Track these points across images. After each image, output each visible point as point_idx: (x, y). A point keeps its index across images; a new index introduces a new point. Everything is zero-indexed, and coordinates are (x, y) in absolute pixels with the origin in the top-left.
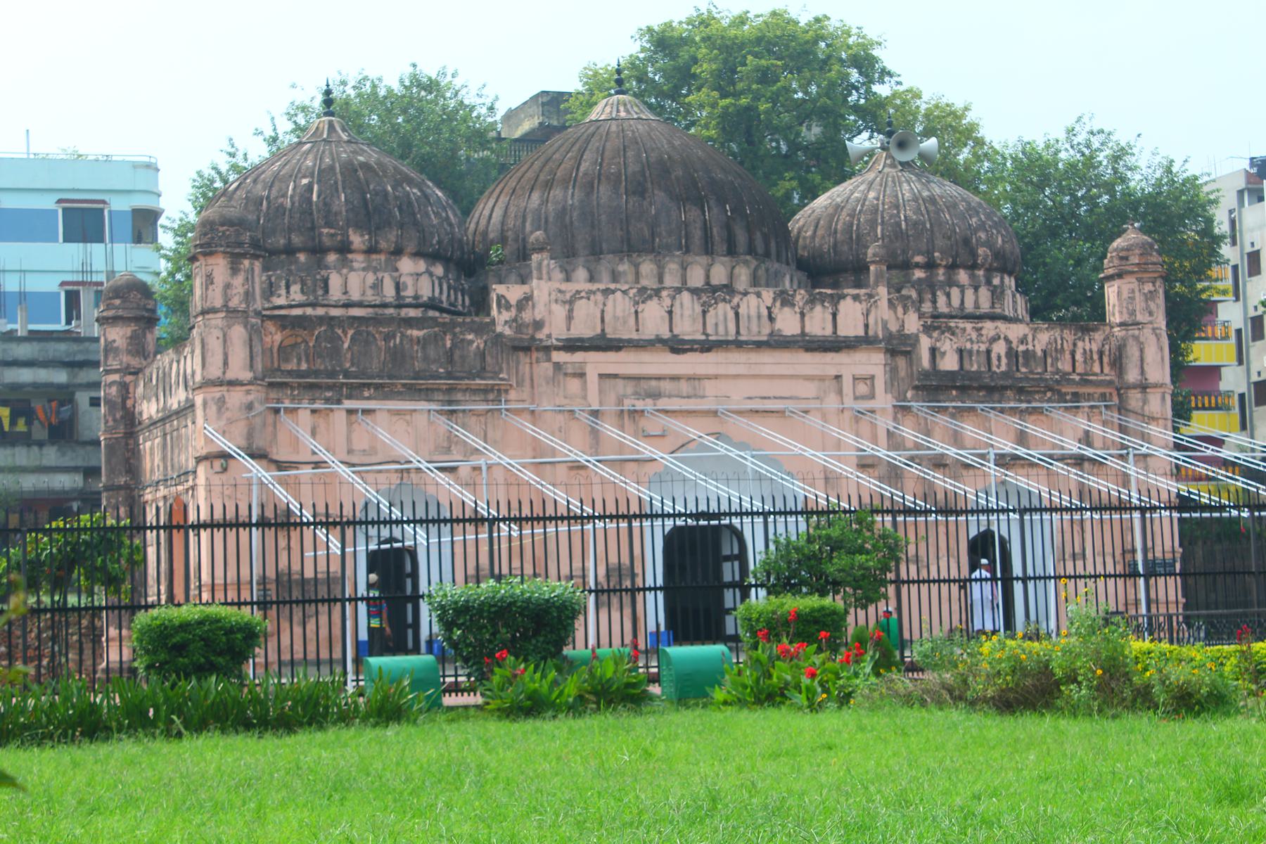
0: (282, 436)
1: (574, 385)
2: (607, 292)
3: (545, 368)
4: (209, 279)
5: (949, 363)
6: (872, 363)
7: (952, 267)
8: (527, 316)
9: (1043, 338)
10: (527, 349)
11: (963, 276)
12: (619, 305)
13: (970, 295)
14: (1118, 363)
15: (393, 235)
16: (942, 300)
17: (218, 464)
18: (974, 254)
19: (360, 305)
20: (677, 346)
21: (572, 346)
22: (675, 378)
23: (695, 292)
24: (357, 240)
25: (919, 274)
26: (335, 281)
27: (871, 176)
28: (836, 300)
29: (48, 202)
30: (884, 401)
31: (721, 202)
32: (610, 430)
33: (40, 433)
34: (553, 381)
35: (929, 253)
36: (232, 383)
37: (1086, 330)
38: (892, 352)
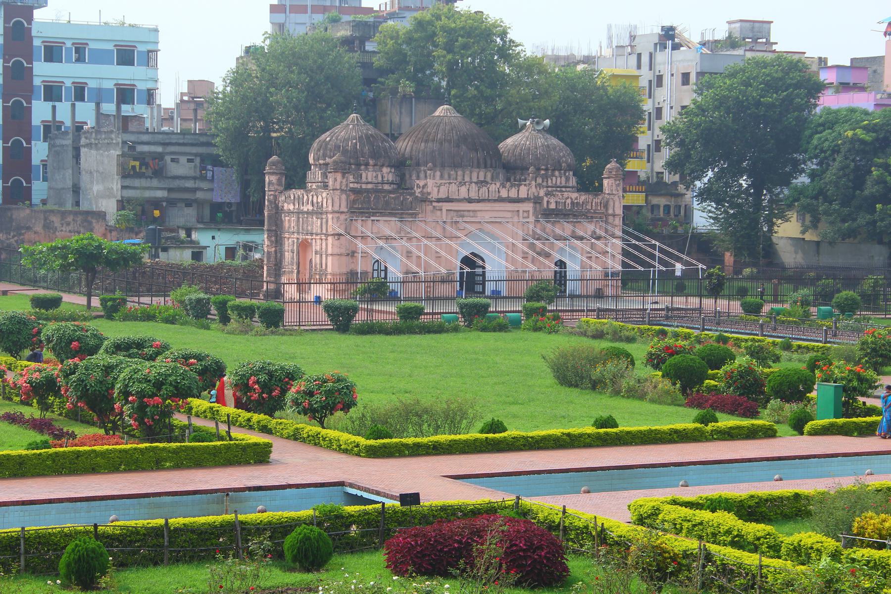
0: (353, 228)
1: (439, 213)
2: (450, 183)
3: (430, 208)
4: (336, 180)
5: (553, 206)
6: (529, 206)
7: (554, 170)
8: (425, 190)
9: (583, 197)
10: (425, 201)
11: (557, 173)
12: (453, 187)
13: (559, 179)
14: (606, 206)
15: (382, 160)
16: (550, 181)
17: (336, 237)
18: (561, 166)
19: (371, 183)
20: (470, 201)
21: (439, 200)
22: (469, 211)
23: (476, 183)
24: (371, 162)
25: (543, 172)
26: (364, 175)
27: (527, 134)
28: (519, 185)
29: (110, 46)
30: (532, 219)
31: (483, 151)
32: (448, 228)
33: (149, 172)
34: (432, 212)
35: (547, 166)
36: (342, 213)
37: (596, 195)
38: (535, 203)
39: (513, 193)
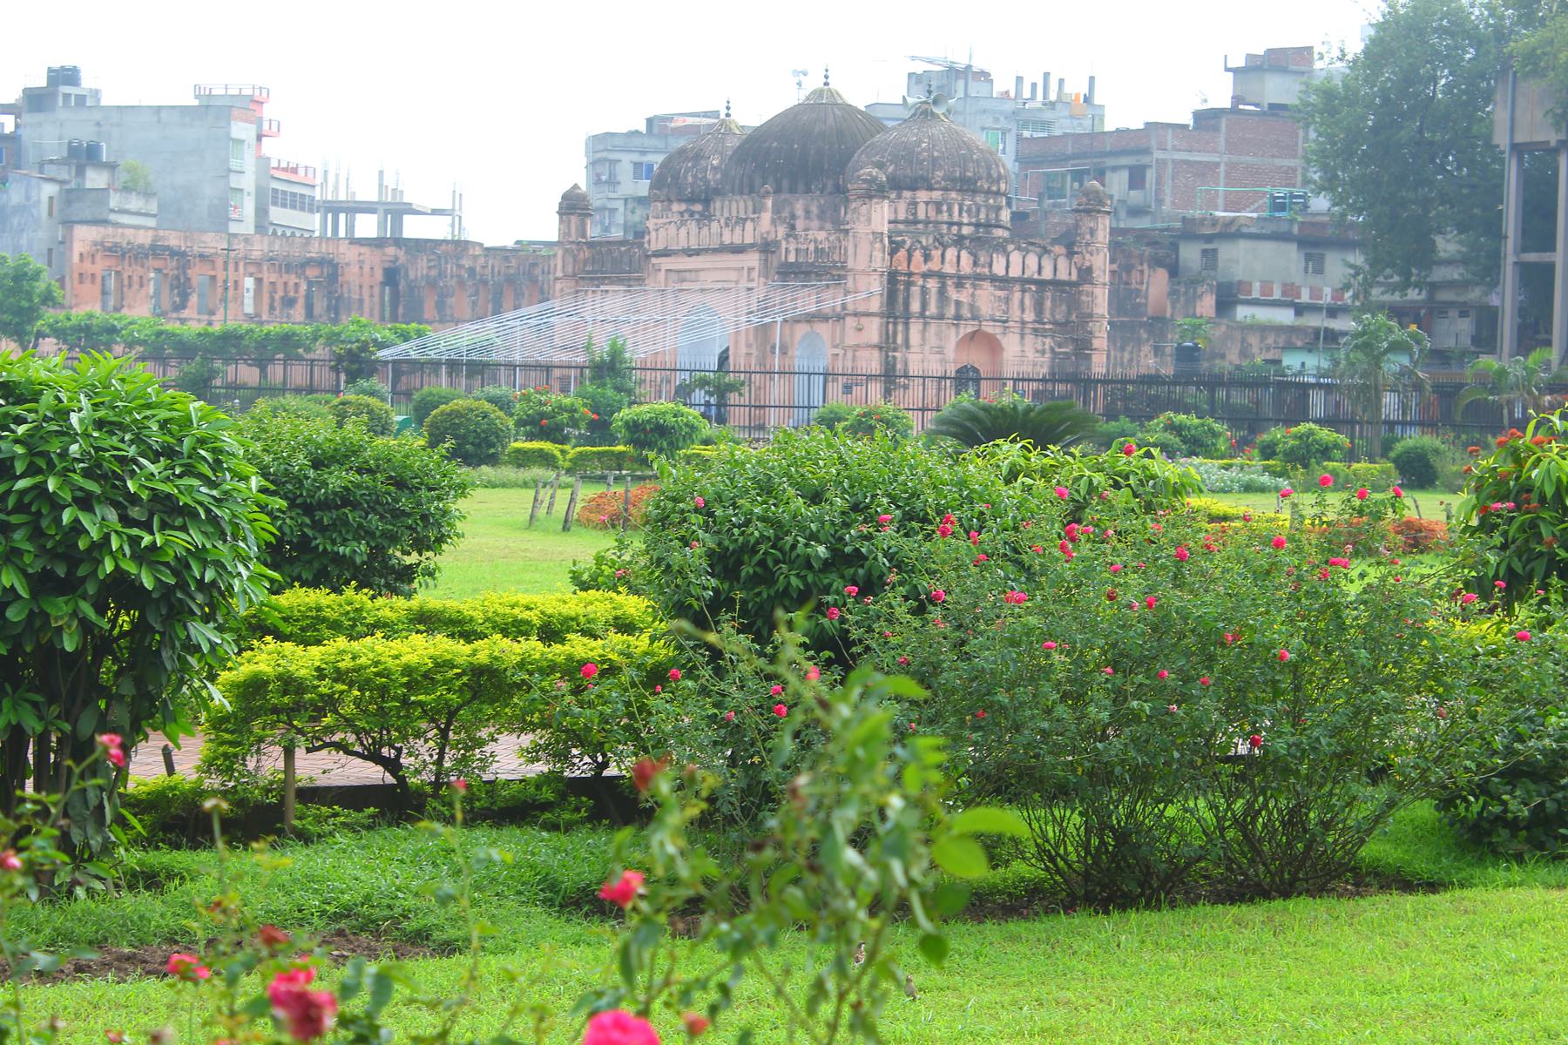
5: (792, 259)
6: (753, 259)
20: (689, 253)
21: (658, 254)
39: (737, 240)
